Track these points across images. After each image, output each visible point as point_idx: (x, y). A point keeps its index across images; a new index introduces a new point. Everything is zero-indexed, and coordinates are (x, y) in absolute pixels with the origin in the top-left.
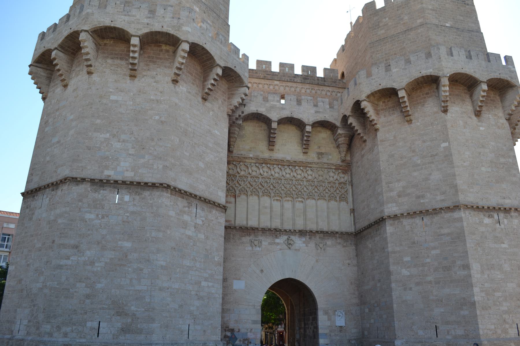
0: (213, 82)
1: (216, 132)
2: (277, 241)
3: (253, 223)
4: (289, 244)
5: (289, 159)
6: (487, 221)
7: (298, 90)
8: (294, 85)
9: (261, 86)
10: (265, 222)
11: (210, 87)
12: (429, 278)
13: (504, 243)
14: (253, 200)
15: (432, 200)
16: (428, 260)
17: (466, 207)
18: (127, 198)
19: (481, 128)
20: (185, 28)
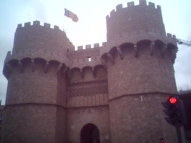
0: (46, 67)
1: (52, 81)
2: (85, 111)
3: (78, 105)
4: (89, 112)
5: (89, 81)
6: (136, 99)
7: (92, 54)
8: (91, 52)
9: (79, 56)
10: (82, 104)
11: (46, 69)
12: (118, 122)
13: (143, 107)
14: (78, 97)
15: (119, 94)
16: (118, 116)
17: (126, 95)
18: (21, 108)
19: (138, 62)
20: (32, 55)
